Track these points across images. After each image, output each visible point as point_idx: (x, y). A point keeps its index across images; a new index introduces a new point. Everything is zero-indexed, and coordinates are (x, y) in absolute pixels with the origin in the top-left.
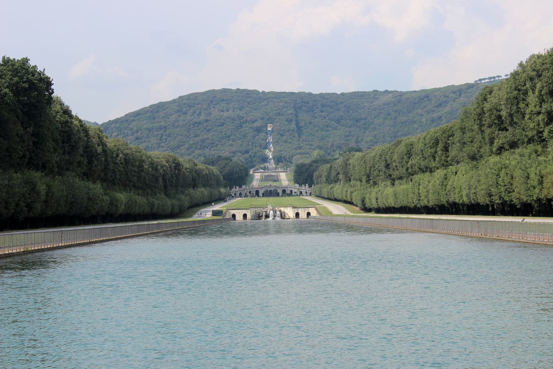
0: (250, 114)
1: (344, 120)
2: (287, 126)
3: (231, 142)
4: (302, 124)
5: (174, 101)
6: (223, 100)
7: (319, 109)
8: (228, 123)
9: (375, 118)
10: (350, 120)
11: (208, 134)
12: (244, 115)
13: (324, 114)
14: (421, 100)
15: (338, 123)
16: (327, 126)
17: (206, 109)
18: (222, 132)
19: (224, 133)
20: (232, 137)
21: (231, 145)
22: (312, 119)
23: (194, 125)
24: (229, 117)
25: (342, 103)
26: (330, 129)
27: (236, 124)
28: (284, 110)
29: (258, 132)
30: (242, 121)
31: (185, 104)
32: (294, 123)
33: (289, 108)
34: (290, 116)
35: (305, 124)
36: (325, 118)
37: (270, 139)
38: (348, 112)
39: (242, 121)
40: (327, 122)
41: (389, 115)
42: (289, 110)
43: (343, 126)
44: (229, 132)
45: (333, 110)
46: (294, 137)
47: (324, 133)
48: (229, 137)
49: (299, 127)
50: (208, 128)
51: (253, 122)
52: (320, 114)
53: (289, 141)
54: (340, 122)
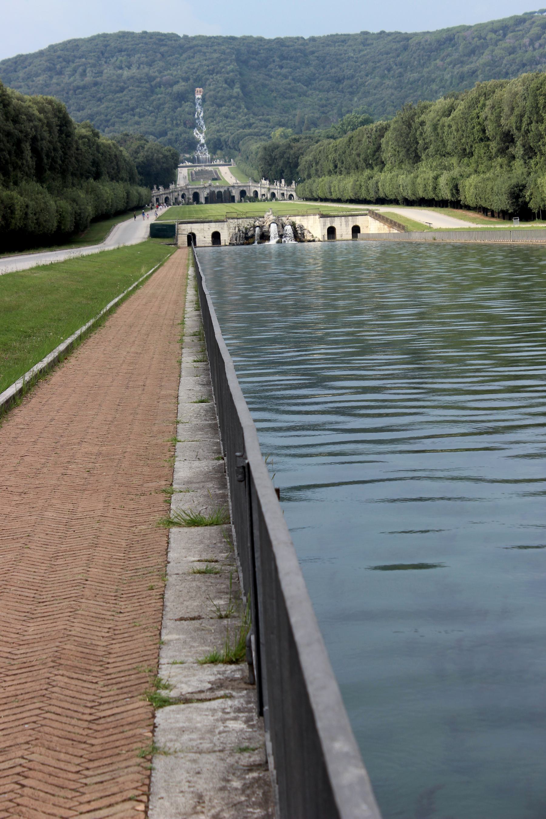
0: (166, 73)
3: (136, 118)
5: (41, 53)
6: (120, 51)
7: (276, 63)
8: (131, 88)
9: (367, 76)
10: (327, 79)
11: (99, 106)
12: (157, 74)
13: (284, 71)
14: (440, 45)
15: (307, 86)
16: (290, 90)
17: (94, 66)
18: (121, 102)
19: (124, 103)
20: (138, 110)
21: (138, 123)
22: (266, 80)
23: (75, 91)
24: (132, 78)
25: (313, 53)
26: (296, 95)
27: (144, 89)
28: (221, 65)
29: (180, 102)
30: (153, 83)
31: (59, 57)
33: (228, 62)
34: (231, 74)
36: (286, 77)
37: (200, 112)
38: (324, 67)
39: (153, 83)
40: (289, 84)
41: (389, 70)
42: (229, 65)
43: (315, 89)
44: (132, 102)
45: (298, 64)
47: (287, 101)
48: (133, 109)
50: (99, 95)
51: (171, 86)
52: (279, 70)
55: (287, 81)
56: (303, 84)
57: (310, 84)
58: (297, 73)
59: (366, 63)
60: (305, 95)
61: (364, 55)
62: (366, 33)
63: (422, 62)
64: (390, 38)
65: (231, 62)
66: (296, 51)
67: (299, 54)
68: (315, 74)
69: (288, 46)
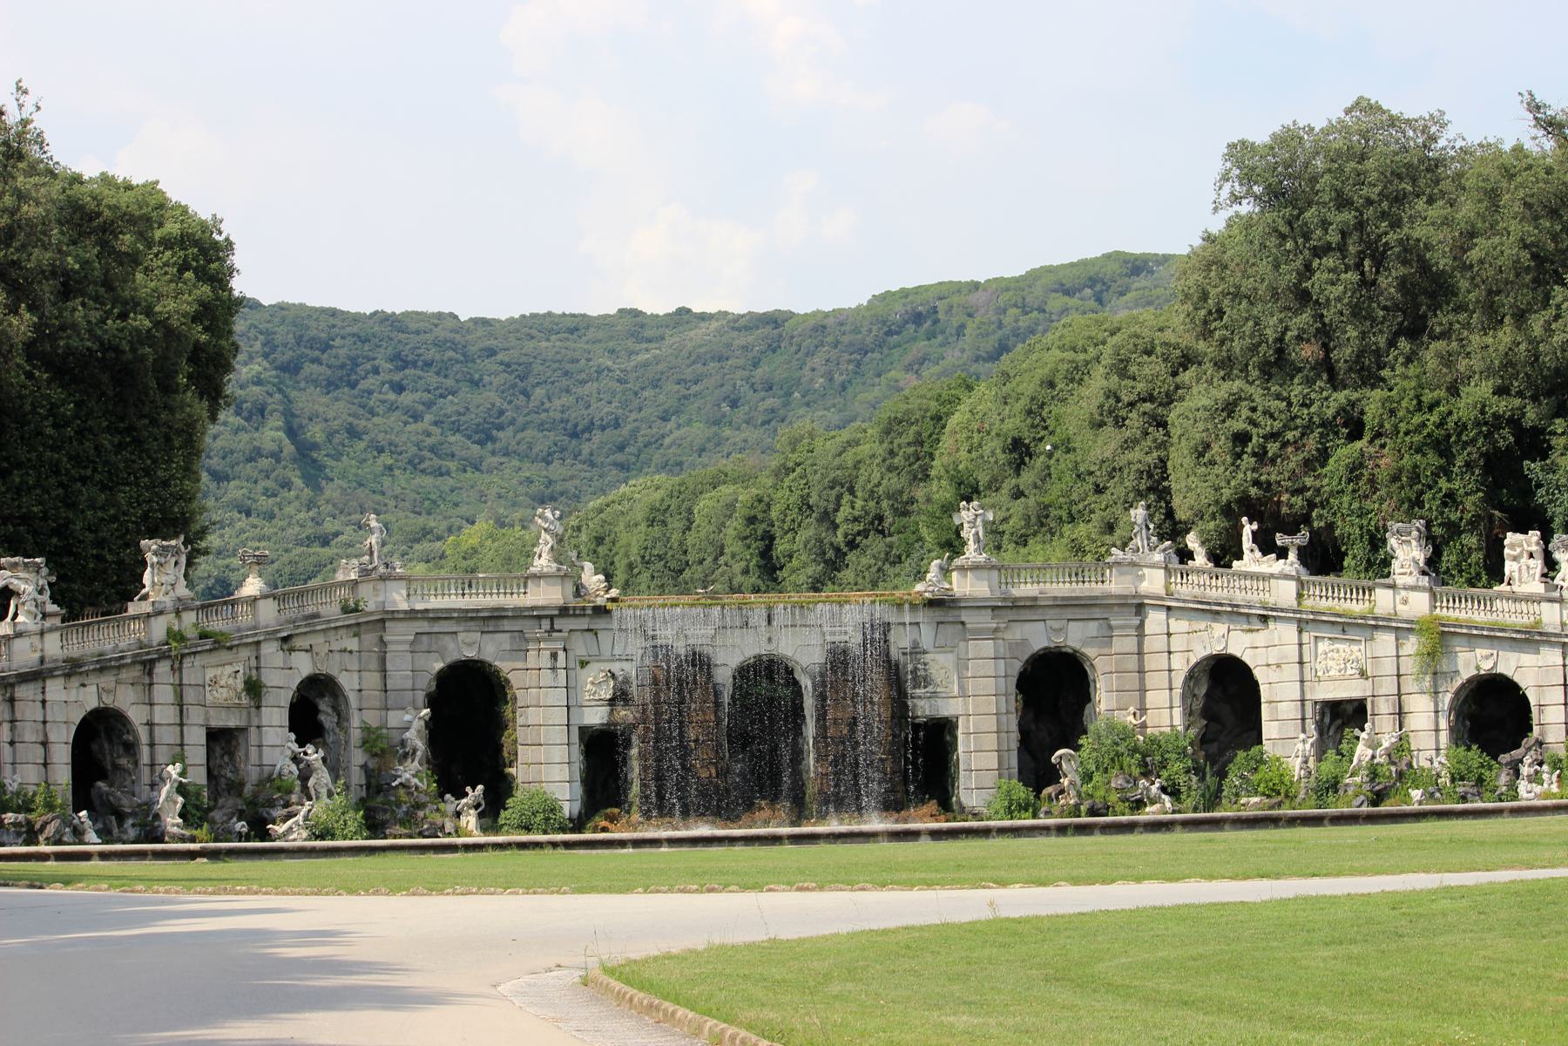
1: (510, 431)
2: (245, 437)
4: (315, 432)
9: (665, 419)
14: (890, 333)
15: (481, 443)
26: (452, 465)
32: (276, 421)
34: (256, 389)
35: (330, 436)
41: (734, 404)
43: (506, 454)
45: (450, 382)
46: (286, 485)
47: (428, 481)
49: (305, 451)
53: (264, 503)
54: (493, 440)
55: (420, 426)
56: (469, 437)
57: (490, 438)
58: (449, 405)
59: (656, 384)
60: (477, 468)
61: (646, 365)
62: (636, 313)
63: (838, 378)
64: (714, 325)
65: (251, 358)
66: (439, 344)
67: (451, 354)
68: (501, 413)
69: (418, 333)
